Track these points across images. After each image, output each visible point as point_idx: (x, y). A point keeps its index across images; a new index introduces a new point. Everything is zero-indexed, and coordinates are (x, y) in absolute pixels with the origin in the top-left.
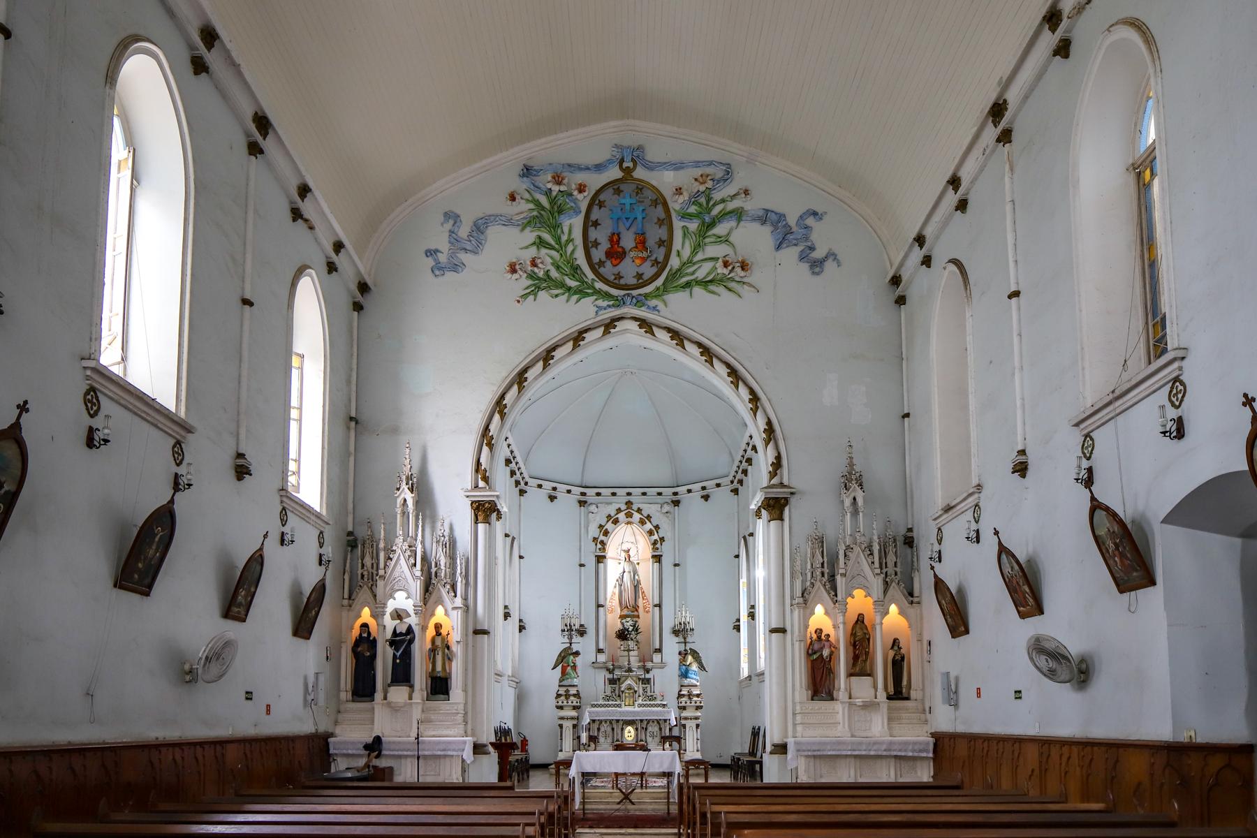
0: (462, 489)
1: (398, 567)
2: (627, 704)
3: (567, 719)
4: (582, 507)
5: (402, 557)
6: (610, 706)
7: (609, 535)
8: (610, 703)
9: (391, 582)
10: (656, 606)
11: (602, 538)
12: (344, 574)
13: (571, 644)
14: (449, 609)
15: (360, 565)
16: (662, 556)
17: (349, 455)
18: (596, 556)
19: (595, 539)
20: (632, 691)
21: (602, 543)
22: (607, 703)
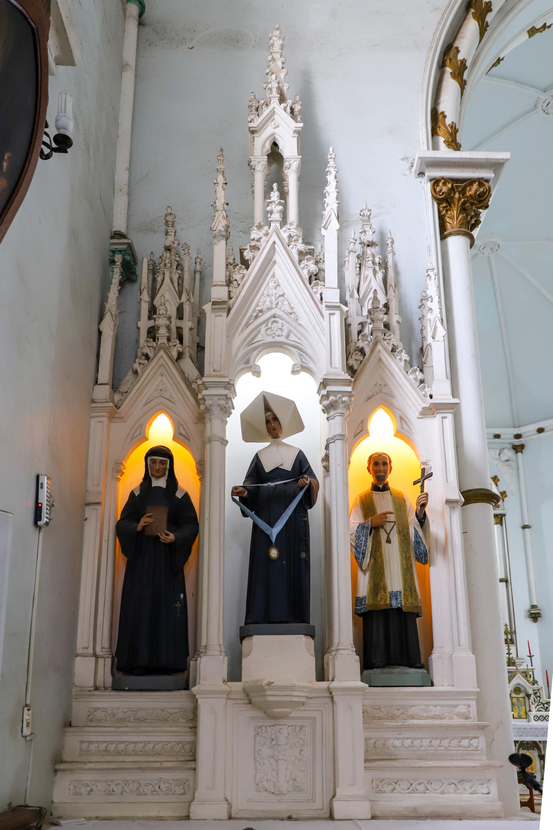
0: (405, 159)
1: (268, 285)
5: (279, 247)
9: (247, 325)
10: (501, 581)
12: (101, 319)
14: (413, 414)
15: (145, 308)
16: (503, 515)
17: (123, 67)
20: (522, 695)
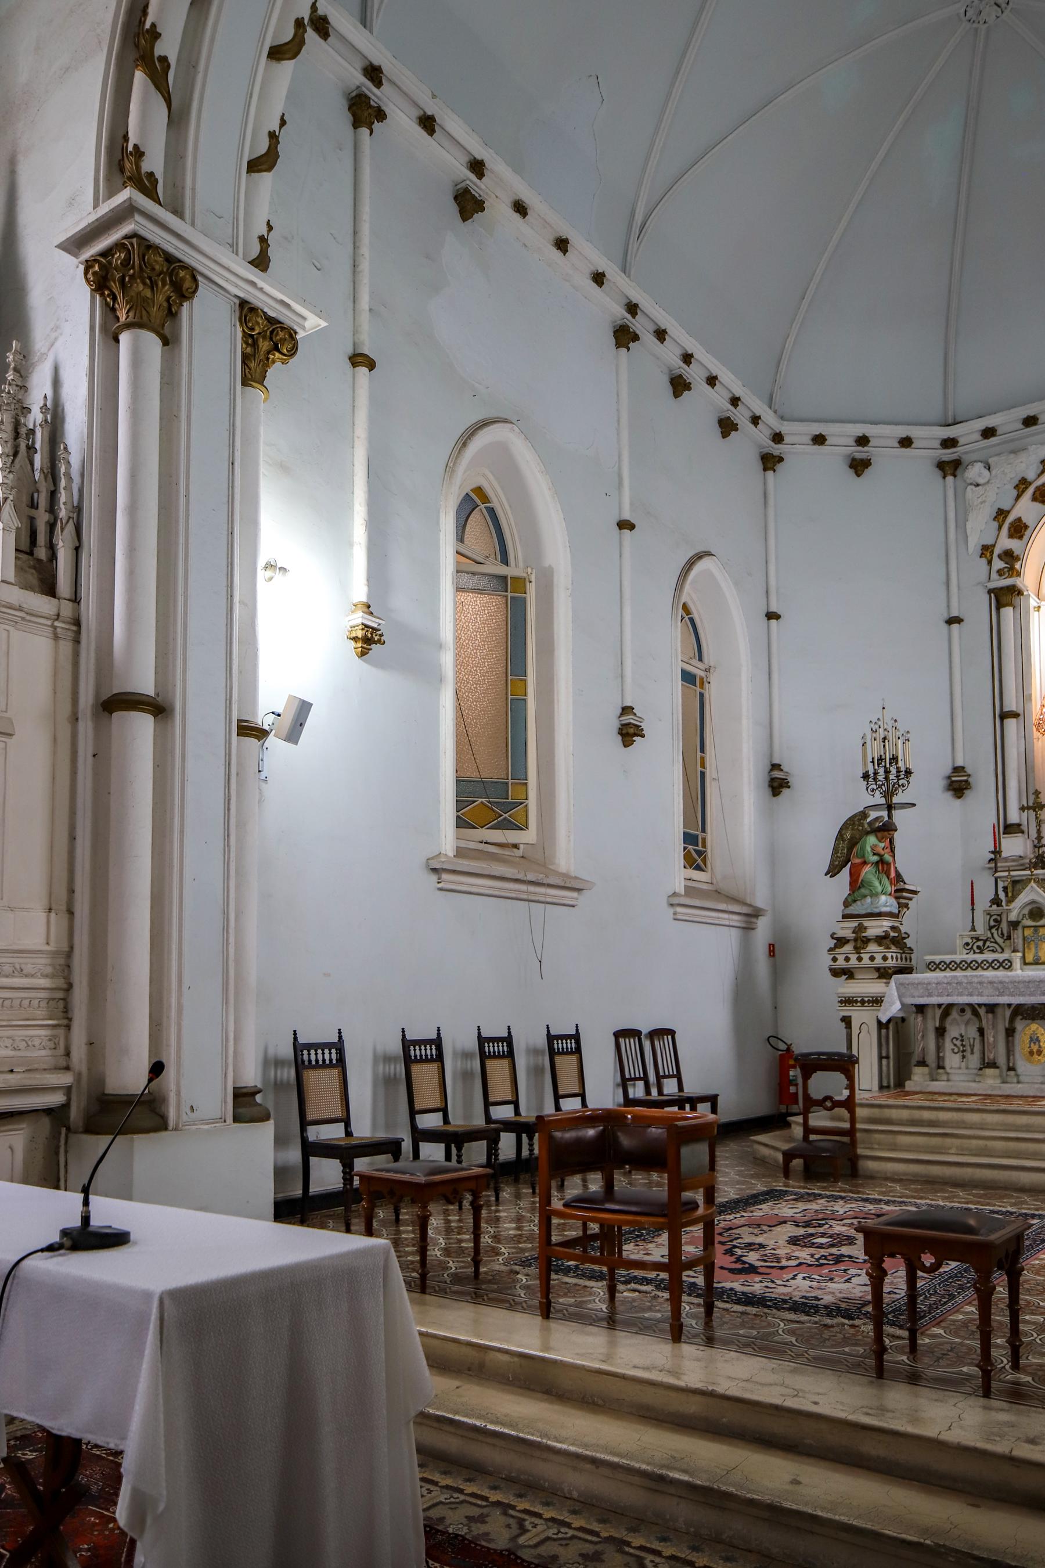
2: (1030, 958)
3: (863, 1002)
4: (950, 479)
6: (979, 965)
7: (1028, 533)
8: (989, 956)
11: (1006, 543)
13: (890, 807)
18: (990, 592)
19: (986, 551)
21: (1009, 556)
22: (979, 957)
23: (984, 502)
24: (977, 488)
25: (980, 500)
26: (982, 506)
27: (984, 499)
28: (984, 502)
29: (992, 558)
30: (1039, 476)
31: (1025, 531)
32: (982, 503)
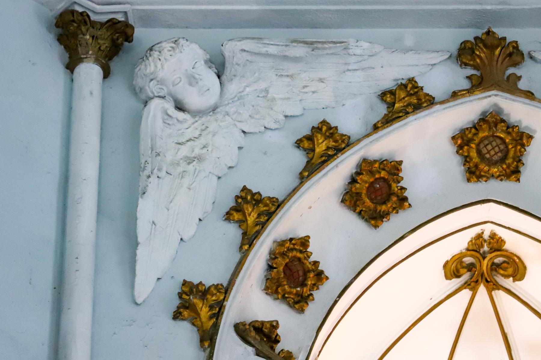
23: (200, 159)
24: (181, 115)
25: (184, 151)
26: (191, 167)
27: (197, 151)
28: (200, 159)
29: (216, 327)
30: (376, 128)
31: (315, 286)
32: (189, 160)
